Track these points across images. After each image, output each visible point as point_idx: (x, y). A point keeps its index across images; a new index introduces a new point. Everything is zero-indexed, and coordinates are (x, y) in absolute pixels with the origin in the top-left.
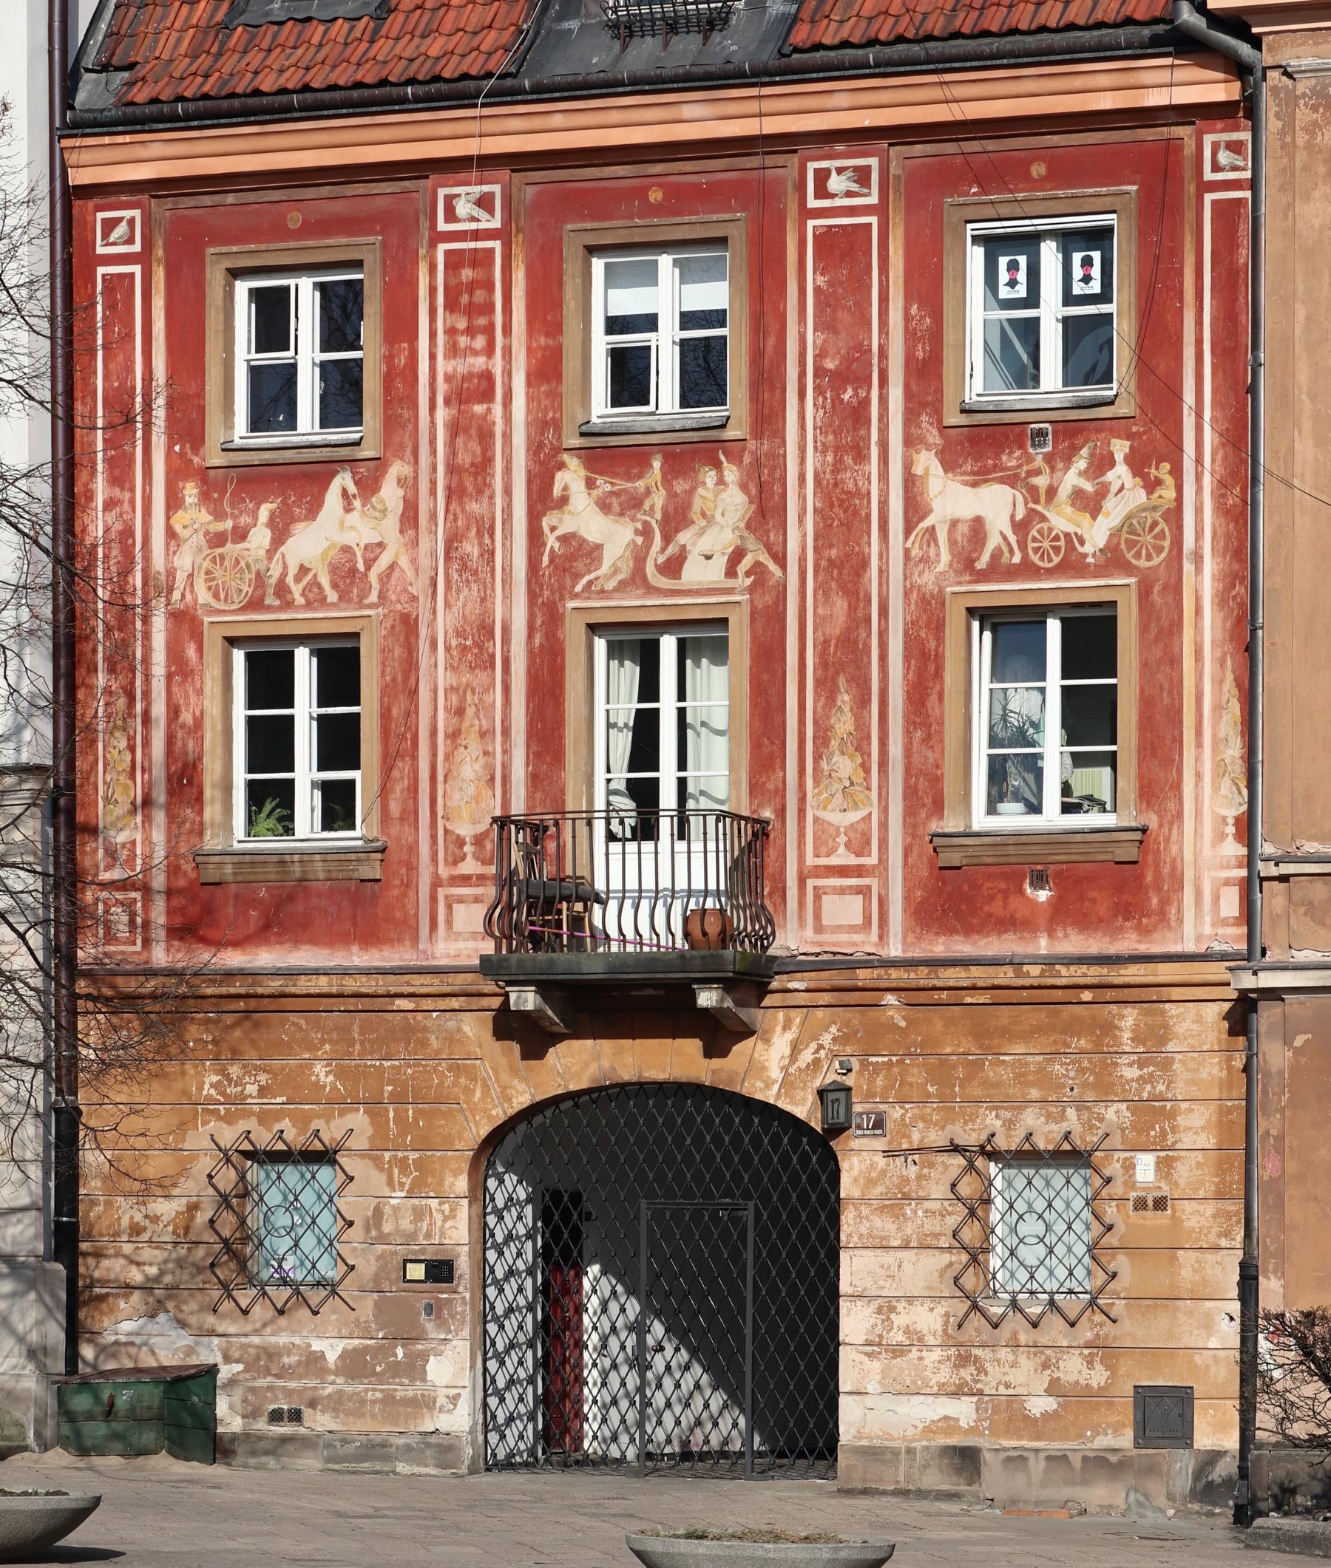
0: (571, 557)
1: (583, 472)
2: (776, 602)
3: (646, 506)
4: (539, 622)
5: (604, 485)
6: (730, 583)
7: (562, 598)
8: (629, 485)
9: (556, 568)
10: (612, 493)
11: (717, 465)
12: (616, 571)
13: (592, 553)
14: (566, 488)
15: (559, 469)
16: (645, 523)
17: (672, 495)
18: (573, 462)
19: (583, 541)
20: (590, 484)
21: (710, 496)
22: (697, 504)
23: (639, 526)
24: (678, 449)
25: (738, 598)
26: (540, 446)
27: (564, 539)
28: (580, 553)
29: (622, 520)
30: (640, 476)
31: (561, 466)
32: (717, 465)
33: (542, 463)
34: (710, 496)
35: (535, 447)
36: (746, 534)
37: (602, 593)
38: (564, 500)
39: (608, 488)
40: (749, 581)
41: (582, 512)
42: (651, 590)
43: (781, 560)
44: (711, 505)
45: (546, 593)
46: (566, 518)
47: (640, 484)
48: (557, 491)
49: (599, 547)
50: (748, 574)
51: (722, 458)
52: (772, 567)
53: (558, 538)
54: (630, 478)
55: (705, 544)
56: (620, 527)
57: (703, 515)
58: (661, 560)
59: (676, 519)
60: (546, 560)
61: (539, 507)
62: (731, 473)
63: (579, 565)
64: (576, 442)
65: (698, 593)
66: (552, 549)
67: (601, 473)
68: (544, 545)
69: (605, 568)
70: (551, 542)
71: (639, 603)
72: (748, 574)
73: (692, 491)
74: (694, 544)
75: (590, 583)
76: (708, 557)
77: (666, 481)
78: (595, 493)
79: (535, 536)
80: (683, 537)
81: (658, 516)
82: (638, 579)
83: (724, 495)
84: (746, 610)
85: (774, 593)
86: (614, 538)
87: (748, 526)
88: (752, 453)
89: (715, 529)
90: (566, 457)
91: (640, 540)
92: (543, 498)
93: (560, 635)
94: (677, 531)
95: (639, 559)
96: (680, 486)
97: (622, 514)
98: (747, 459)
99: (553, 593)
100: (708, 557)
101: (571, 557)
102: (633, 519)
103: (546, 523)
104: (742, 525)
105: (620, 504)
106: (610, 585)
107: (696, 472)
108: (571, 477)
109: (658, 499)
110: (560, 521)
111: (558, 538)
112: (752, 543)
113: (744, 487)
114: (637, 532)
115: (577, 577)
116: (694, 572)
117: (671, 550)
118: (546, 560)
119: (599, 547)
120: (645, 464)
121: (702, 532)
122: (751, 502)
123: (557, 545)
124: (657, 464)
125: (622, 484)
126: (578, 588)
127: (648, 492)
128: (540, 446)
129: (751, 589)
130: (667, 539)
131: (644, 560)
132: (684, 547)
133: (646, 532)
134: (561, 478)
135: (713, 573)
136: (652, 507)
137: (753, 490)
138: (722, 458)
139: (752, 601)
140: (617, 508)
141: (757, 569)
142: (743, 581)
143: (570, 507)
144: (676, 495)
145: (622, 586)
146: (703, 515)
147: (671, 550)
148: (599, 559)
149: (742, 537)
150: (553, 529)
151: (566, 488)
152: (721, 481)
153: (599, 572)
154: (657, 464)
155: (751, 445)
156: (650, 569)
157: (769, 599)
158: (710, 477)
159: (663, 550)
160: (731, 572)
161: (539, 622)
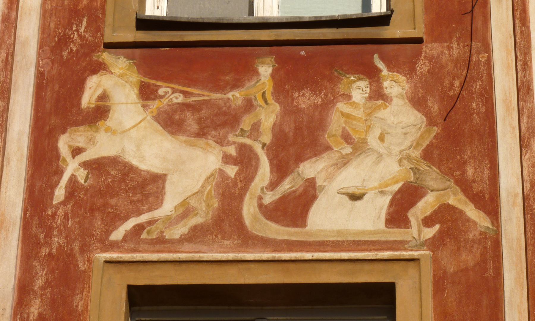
0: (108, 191)
1: (135, 78)
2: (483, 262)
3: (246, 123)
4: (39, 282)
5: (170, 95)
6: (396, 234)
7: (85, 249)
8: (215, 96)
9: (78, 205)
10: (186, 106)
11: (372, 74)
12: (185, 211)
13: (147, 187)
14: (104, 97)
15: (94, 72)
16: (243, 149)
17: (290, 110)
18: (119, 63)
19: (128, 170)
20: (146, 93)
21: (359, 113)
22: (335, 123)
23: (232, 151)
24: (303, 52)
25: (415, 254)
26: (64, 41)
27: (96, 166)
28: (124, 186)
29: (202, 142)
30: (236, 85)
31: (99, 67)
32: (372, 74)
33: (63, 64)
34: (359, 113)
35: (53, 42)
36: (424, 166)
37: (161, 242)
38: (100, 112)
39: (179, 99)
40: (430, 232)
41: (130, 127)
42: (248, 239)
43: (490, 203)
44: (361, 126)
45: (57, 241)
46: (102, 137)
47: (236, 96)
48: (88, 99)
49: (158, 179)
50: (428, 222)
51: (380, 64)
52: (472, 212)
53: (85, 165)
54: (218, 88)
55: (351, 177)
56: (197, 153)
57: (347, 138)
58: (269, 198)
59: (298, 142)
60: (60, 193)
61: (55, 121)
62: (395, 85)
63: (119, 202)
64: (131, 35)
65: (337, 246)
66: (73, 179)
67: (167, 79)
68: (59, 173)
69: (168, 207)
70: (72, 168)
71: (231, 256)
72: (428, 222)
73: (327, 105)
74: (330, 178)
75: (139, 229)
76: (355, 197)
77: (283, 86)
78: (154, 105)
79: (43, 161)
80: (310, 169)
81: (267, 138)
82: (227, 221)
83: (383, 113)
84: (428, 271)
85: (477, 250)
86: (187, 170)
87: (427, 155)
88: (431, 59)
89: (367, 161)
90: (106, 57)
91: (232, 171)
92: (61, 106)
93: (78, 302)
94: (300, 159)
95: (230, 195)
96: (306, 100)
97: (201, 134)
98: (423, 67)
99: (69, 239)
100: (355, 197)
101: (108, 191)
102: (221, 142)
103: (64, 144)
104: (416, 153)
105: (200, 121)
106: (178, 231)
107: (334, 80)
108: (116, 83)
109: (269, 116)
110: (91, 141)
111: (85, 165)
112: (433, 177)
113: (418, 102)
114: (227, 159)
115: (118, 218)
116: (328, 218)
117: (286, 186)
118: (60, 193)
119: (158, 179)
120: (245, 71)
121: (344, 162)
122: (431, 122)
123: (82, 175)
124: (265, 71)
125: (200, 94)
126: (117, 235)
127: (249, 105)
128: (64, 41)
129: (434, 244)
130: (281, 170)
131: (240, 198)
132: (311, 183)
133: (245, 160)
134: (93, 88)
135: (368, 219)
136: (256, 127)
137: (435, 107)
138: (380, 64)
139: (435, 261)
140: (194, 127)
141: (444, 215)
142: (419, 231)
143: (109, 123)
144: (298, 111)
145: (196, 235)
146: (347, 138)
147: (286, 186)
148: (158, 198)
149: (416, 171)
150: (76, 151)
151: (104, 97)
152: (378, 95)
153: (158, 213)
154: (265, 71)
155: (431, 49)
156: (249, 210)
157: (469, 259)
158: (359, 90)
159: (273, 186)
160: (397, 216)
161: (39, 282)
